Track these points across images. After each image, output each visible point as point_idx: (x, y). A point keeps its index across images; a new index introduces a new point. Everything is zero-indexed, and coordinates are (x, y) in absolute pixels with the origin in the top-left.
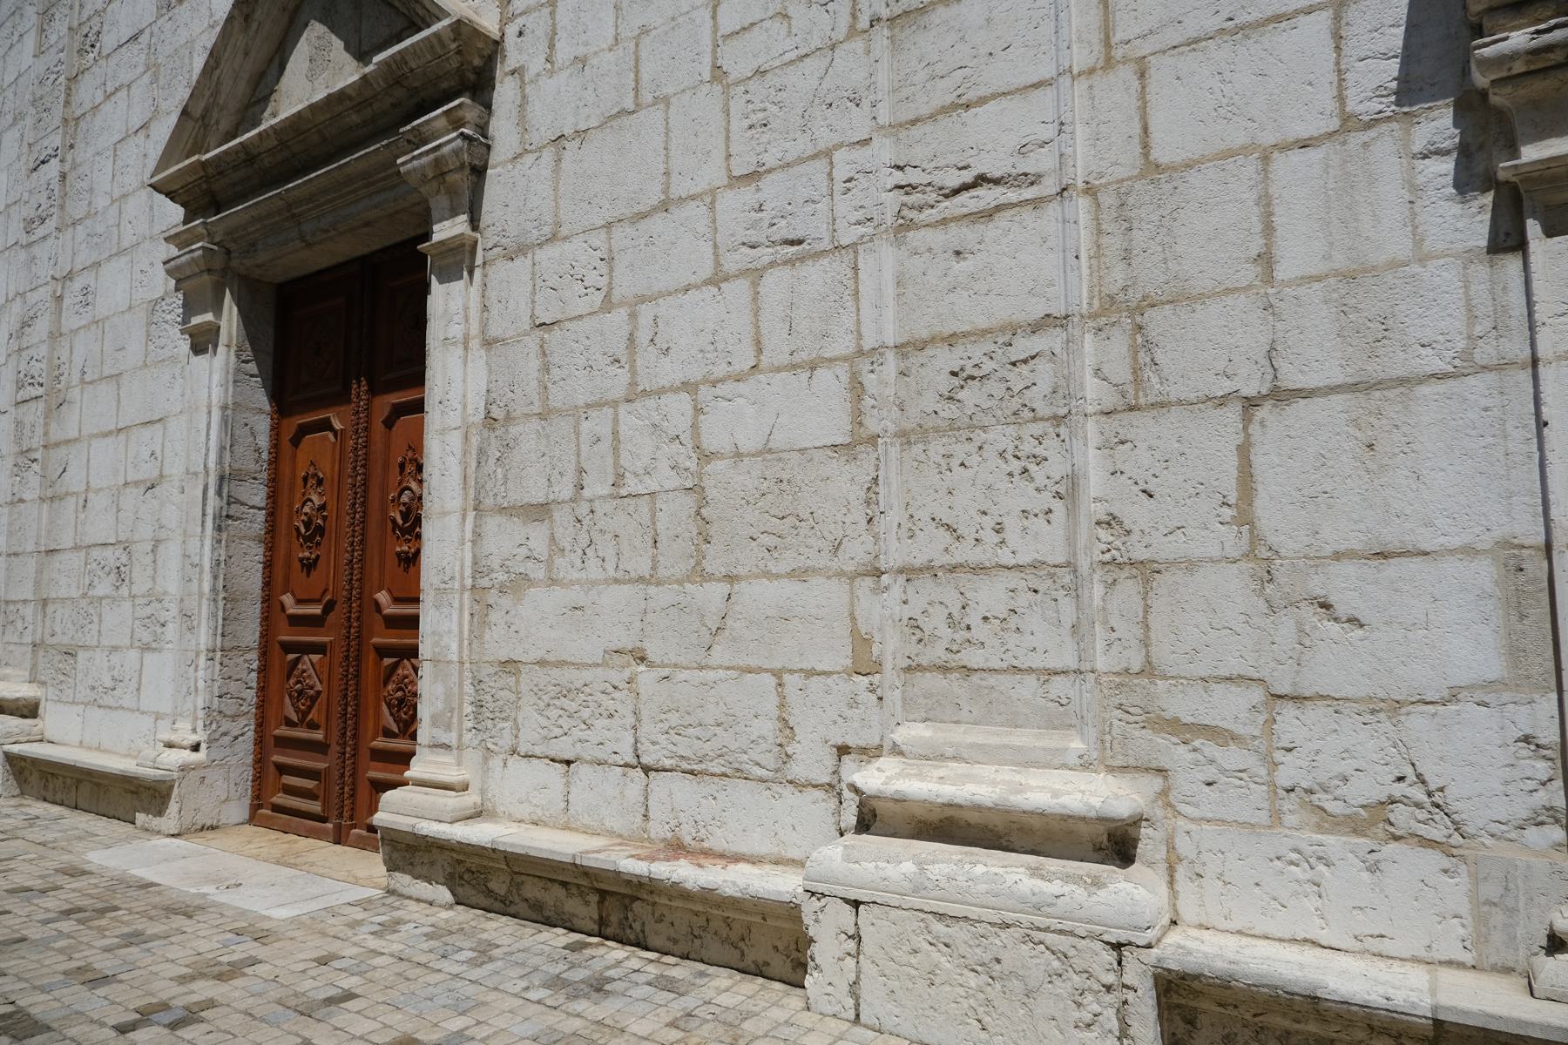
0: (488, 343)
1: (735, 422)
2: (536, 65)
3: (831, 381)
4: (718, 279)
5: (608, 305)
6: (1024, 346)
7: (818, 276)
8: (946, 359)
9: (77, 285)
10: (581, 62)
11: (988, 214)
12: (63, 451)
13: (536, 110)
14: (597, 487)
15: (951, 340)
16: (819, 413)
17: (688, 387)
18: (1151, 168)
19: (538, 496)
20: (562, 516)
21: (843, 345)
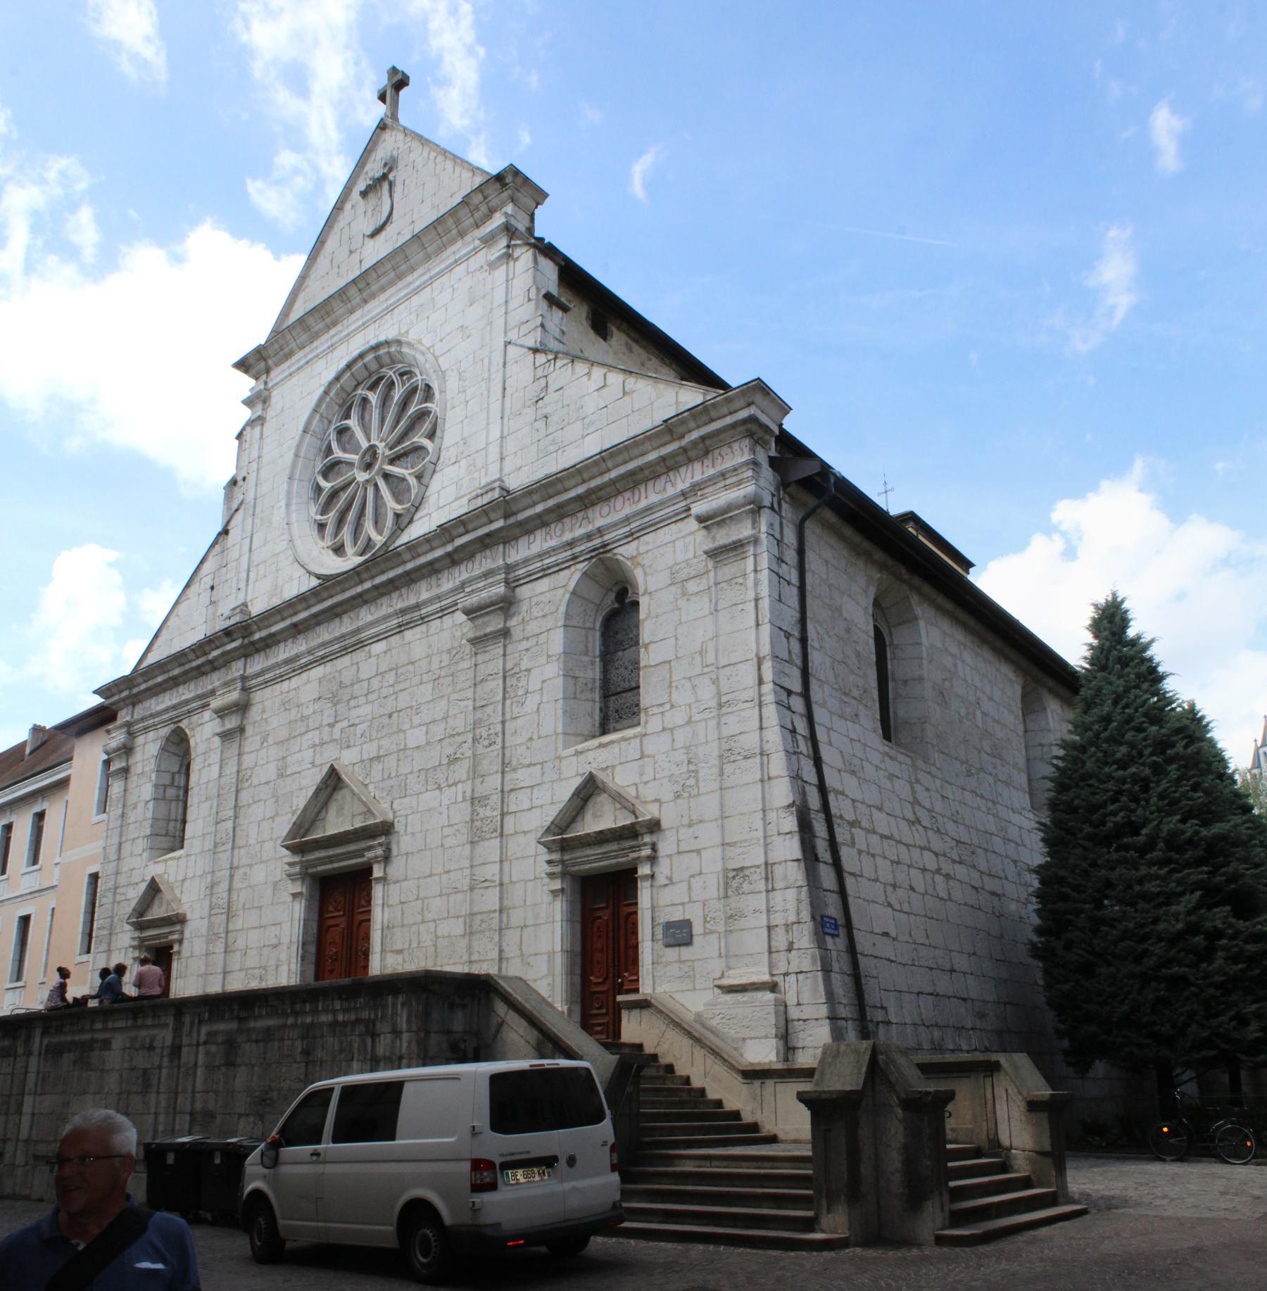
0: (389, 906)
2: (402, 832)
3: (461, 920)
4: (441, 895)
7: (460, 896)
9: (241, 871)
10: (413, 834)
13: (402, 844)
14: (414, 945)
15: (481, 913)
16: (458, 928)
17: (434, 921)
18: (511, 882)
19: (400, 947)
20: (406, 953)
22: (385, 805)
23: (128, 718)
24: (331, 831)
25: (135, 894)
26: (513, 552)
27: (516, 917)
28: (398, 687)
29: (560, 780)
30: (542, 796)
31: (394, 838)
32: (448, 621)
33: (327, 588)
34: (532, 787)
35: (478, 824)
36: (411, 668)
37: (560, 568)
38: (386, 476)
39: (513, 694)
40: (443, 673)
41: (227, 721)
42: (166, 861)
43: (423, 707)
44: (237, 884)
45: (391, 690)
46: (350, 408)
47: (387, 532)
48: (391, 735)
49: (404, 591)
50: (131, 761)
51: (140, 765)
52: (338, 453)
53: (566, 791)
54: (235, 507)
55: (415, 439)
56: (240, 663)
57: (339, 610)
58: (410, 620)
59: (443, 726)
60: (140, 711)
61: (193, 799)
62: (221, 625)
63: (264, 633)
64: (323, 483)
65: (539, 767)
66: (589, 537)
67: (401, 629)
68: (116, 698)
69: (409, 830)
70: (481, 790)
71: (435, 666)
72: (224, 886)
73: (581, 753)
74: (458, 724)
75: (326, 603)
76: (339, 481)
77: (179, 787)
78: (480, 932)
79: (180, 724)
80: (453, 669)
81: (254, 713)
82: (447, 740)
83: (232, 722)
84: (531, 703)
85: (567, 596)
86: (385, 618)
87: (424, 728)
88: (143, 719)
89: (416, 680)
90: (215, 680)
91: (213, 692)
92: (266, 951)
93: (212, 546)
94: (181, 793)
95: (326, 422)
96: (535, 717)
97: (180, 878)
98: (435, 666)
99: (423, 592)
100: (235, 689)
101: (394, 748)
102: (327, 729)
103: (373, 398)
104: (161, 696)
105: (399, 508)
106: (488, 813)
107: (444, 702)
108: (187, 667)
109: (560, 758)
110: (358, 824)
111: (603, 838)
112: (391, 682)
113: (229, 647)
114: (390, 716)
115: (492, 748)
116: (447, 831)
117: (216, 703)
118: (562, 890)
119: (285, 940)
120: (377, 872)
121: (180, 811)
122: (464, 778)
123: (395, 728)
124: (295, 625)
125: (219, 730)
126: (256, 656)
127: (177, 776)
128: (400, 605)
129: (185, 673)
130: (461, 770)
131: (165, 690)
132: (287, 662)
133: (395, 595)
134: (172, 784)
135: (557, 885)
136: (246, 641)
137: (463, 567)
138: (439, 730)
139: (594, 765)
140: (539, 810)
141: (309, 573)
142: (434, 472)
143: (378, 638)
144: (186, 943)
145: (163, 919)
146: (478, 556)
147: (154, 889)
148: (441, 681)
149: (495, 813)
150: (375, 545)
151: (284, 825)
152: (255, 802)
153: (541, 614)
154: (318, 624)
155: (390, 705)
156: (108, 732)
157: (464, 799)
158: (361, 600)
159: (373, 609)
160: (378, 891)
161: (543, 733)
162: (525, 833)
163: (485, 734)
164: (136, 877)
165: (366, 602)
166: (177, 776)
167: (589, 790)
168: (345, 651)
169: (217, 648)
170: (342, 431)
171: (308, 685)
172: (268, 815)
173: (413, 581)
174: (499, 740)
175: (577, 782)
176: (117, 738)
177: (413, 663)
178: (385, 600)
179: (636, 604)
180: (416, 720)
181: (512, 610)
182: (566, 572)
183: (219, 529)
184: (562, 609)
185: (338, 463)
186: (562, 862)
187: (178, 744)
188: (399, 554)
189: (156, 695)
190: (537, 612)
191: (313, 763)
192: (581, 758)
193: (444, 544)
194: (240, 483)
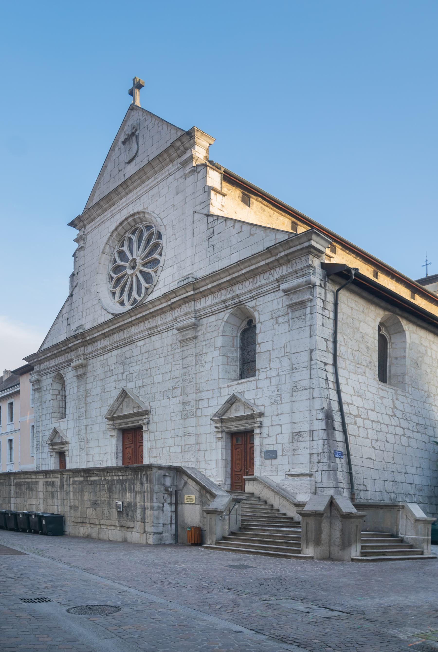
0: (150, 441)
1: (173, 450)
3: (180, 447)
4: (171, 438)
5: (162, 439)
6: (193, 446)
8: (187, 446)
11: (190, 436)
12: (89, 449)
16: (179, 450)
17: (169, 447)
18: (200, 434)
19: (155, 455)
20: (158, 458)
21: (181, 444)
22: (147, 404)
23: (38, 369)
24: (125, 413)
25: (49, 433)
26: (198, 305)
27: (203, 447)
28: (149, 359)
29: (221, 396)
30: (213, 402)
31: (151, 416)
32: (170, 333)
33: (116, 319)
34: (209, 399)
35: (186, 412)
36: (155, 351)
37: (219, 311)
38: (141, 272)
39: (199, 363)
40: (169, 354)
41: (78, 370)
42: (59, 422)
43: (161, 367)
44: (88, 431)
45: (147, 360)
46: (123, 242)
47: (142, 296)
48: (147, 378)
49: (150, 320)
50: (41, 385)
51: (45, 387)
52: (119, 262)
53: (223, 401)
54: (74, 285)
55: (153, 256)
56: (82, 349)
57: (122, 328)
58: (152, 333)
59: (170, 375)
60: (43, 366)
61: (68, 400)
62: (72, 334)
63: (91, 337)
64: (113, 275)
65: (211, 391)
66: (233, 298)
67: (150, 336)
68: (32, 361)
69: (157, 413)
70: (187, 399)
71: (165, 351)
72: (84, 431)
73: (230, 386)
74: (176, 374)
75: (116, 325)
76: (120, 275)
77: (62, 395)
78: (188, 451)
79: (60, 372)
80: (173, 352)
81: (89, 368)
82: (172, 380)
83: (80, 371)
84: (208, 366)
85: (223, 323)
86: (142, 331)
87: (162, 375)
88: (44, 370)
89: (158, 356)
90: (72, 355)
91: (71, 360)
92: (102, 455)
93: (66, 301)
94: (63, 397)
95: (113, 249)
96: (209, 371)
97: (66, 428)
98: (165, 351)
99: (159, 320)
100: (81, 359)
101: (149, 383)
102: (120, 375)
103: (134, 238)
104: (51, 361)
105: (147, 285)
106: (190, 408)
107: (170, 365)
108: (60, 350)
109: (221, 388)
110: (136, 411)
111: (239, 419)
112: (147, 357)
113: (76, 342)
114: (147, 370)
115: (191, 383)
116: (172, 414)
117: (73, 364)
118: (222, 437)
119: (109, 451)
120: (145, 428)
121: (64, 404)
122: (179, 395)
123: (149, 375)
124: (104, 334)
125: (75, 375)
126: (89, 346)
127: (61, 391)
128: (149, 326)
129: (59, 352)
130: (178, 392)
131: (52, 359)
132: (101, 348)
133: (147, 322)
134: (59, 394)
135: (220, 435)
136: (84, 340)
137: (176, 311)
138: (168, 376)
139: (236, 391)
140: (212, 408)
141: (108, 312)
142: (162, 270)
143: (140, 340)
144: (70, 451)
145: (60, 442)
146: (183, 306)
147: (55, 432)
148: (168, 357)
149: (193, 408)
150: (137, 301)
151: (105, 410)
152: (93, 402)
153: (212, 330)
154: (114, 333)
155: (147, 366)
156: (31, 374)
157: (180, 403)
158: (131, 324)
159: (137, 327)
160: (145, 436)
161: (213, 378)
162: (206, 416)
163: (188, 378)
164: (48, 427)
165: (134, 325)
166: (61, 391)
167: (233, 400)
168: (126, 344)
169: (72, 343)
170: (121, 254)
171: (112, 358)
172: (99, 406)
173: (154, 316)
174: (194, 381)
175: (227, 397)
176: (35, 377)
177: (156, 350)
178: (142, 324)
179: (255, 326)
180: (158, 372)
181: (199, 329)
182: (223, 313)
183: (69, 295)
184: (221, 329)
185: (119, 266)
186: (222, 427)
187: (60, 379)
188: (147, 305)
189: (49, 360)
190: (209, 330)
191: (116, 388)
192: (230, 388)
193: (167, 301)
194: (76, 275)
